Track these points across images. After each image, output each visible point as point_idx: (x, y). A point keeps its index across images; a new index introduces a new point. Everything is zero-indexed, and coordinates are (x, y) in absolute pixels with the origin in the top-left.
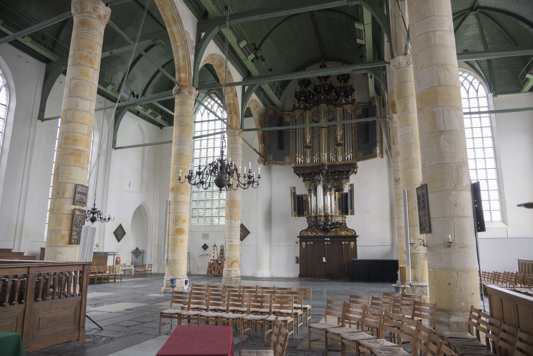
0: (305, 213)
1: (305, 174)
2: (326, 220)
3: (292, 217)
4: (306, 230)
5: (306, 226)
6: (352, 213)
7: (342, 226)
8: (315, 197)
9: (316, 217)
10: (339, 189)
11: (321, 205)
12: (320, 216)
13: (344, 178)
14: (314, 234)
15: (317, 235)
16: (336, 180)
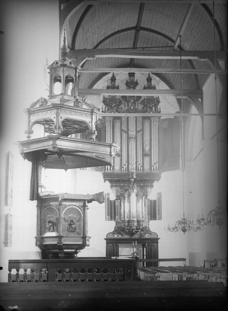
0: (117, 217)
1: (113, 180)
2: (138, 225)
3: (106, 221)
4: (113, 233)
5: (112, 230)
6: (161, 220)
7: (146, 230)
8: (128, 204)
9: (129, 221)
10: (145, 195)
11: (134, 212)
12: (134, 221)
13: (149, 186)
14: (120, 236)
15: (123, 237)
16: (142, 187)
